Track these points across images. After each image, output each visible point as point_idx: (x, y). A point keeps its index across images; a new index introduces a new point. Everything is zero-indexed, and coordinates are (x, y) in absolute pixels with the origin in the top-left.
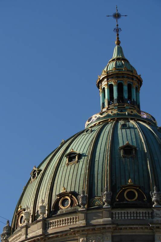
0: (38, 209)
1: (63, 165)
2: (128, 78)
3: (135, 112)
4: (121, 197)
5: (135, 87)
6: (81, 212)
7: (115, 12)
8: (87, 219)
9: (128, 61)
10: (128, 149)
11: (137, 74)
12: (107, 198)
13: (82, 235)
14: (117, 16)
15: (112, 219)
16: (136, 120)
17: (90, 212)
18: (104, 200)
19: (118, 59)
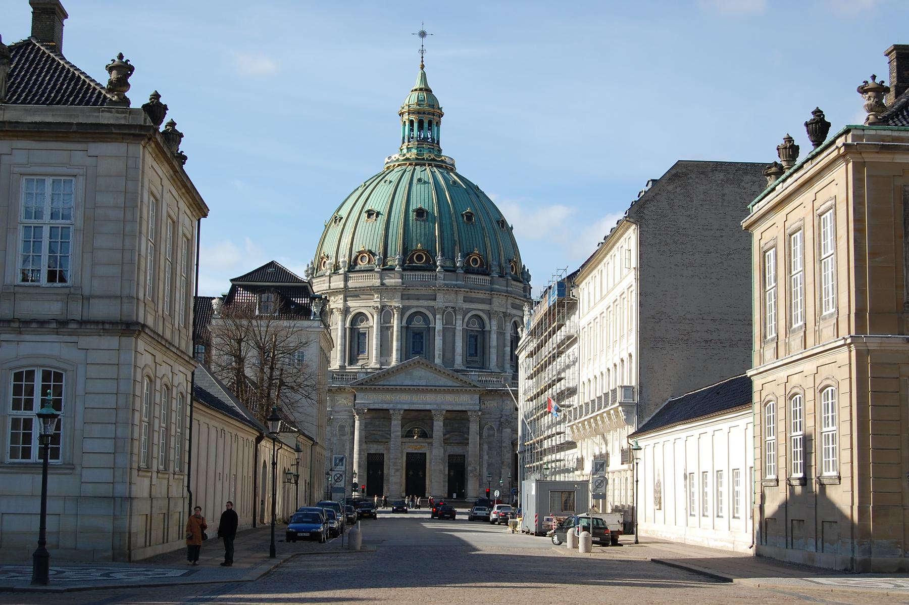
0: (341, 260)
1: (363, 220)
2: (429, 114)
3: (432, 156)
4: (411, 261)
5: (435, 124)
6: (377, 272)
7: (420, 29)
8: (382, 279)
9: (431, 91)
10: (420, 213)
11: (439, 107)
12: (399, 262)
13: (377, 293)
14: (423, 34)
15: (402, 280)
16: (433, 165)
17: (384, 272)
18: (397, 263)
19: (421, 89)
